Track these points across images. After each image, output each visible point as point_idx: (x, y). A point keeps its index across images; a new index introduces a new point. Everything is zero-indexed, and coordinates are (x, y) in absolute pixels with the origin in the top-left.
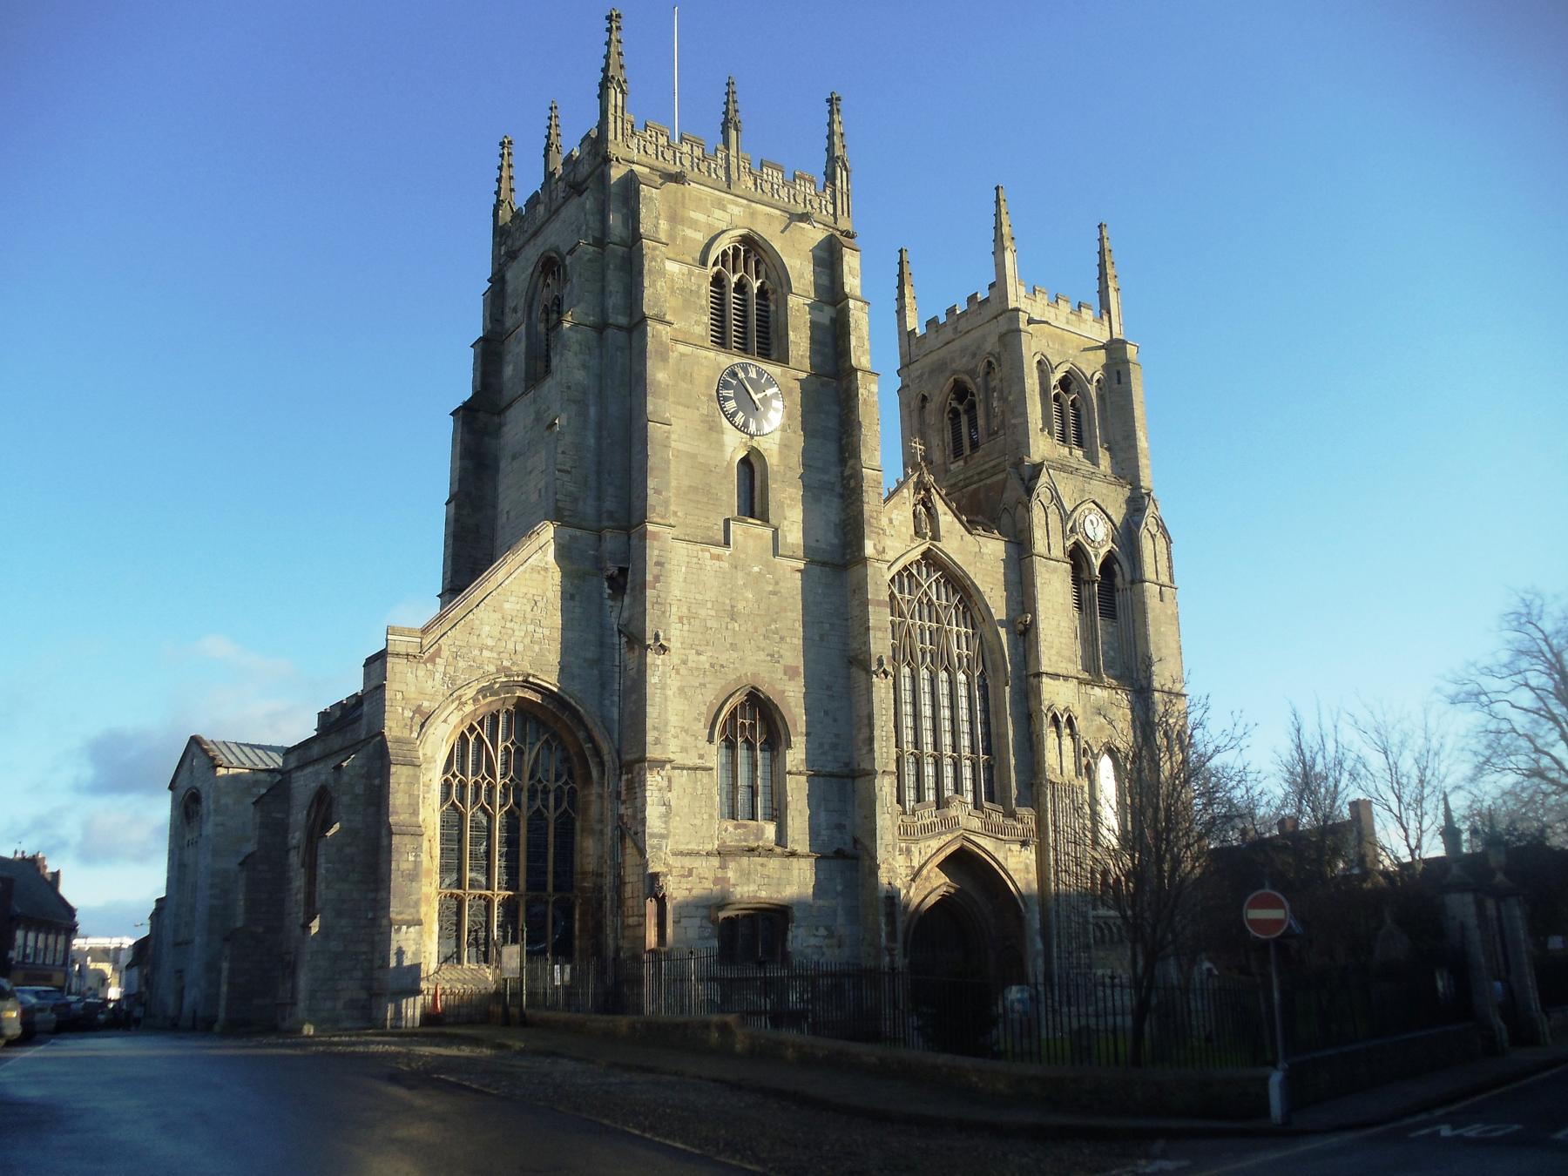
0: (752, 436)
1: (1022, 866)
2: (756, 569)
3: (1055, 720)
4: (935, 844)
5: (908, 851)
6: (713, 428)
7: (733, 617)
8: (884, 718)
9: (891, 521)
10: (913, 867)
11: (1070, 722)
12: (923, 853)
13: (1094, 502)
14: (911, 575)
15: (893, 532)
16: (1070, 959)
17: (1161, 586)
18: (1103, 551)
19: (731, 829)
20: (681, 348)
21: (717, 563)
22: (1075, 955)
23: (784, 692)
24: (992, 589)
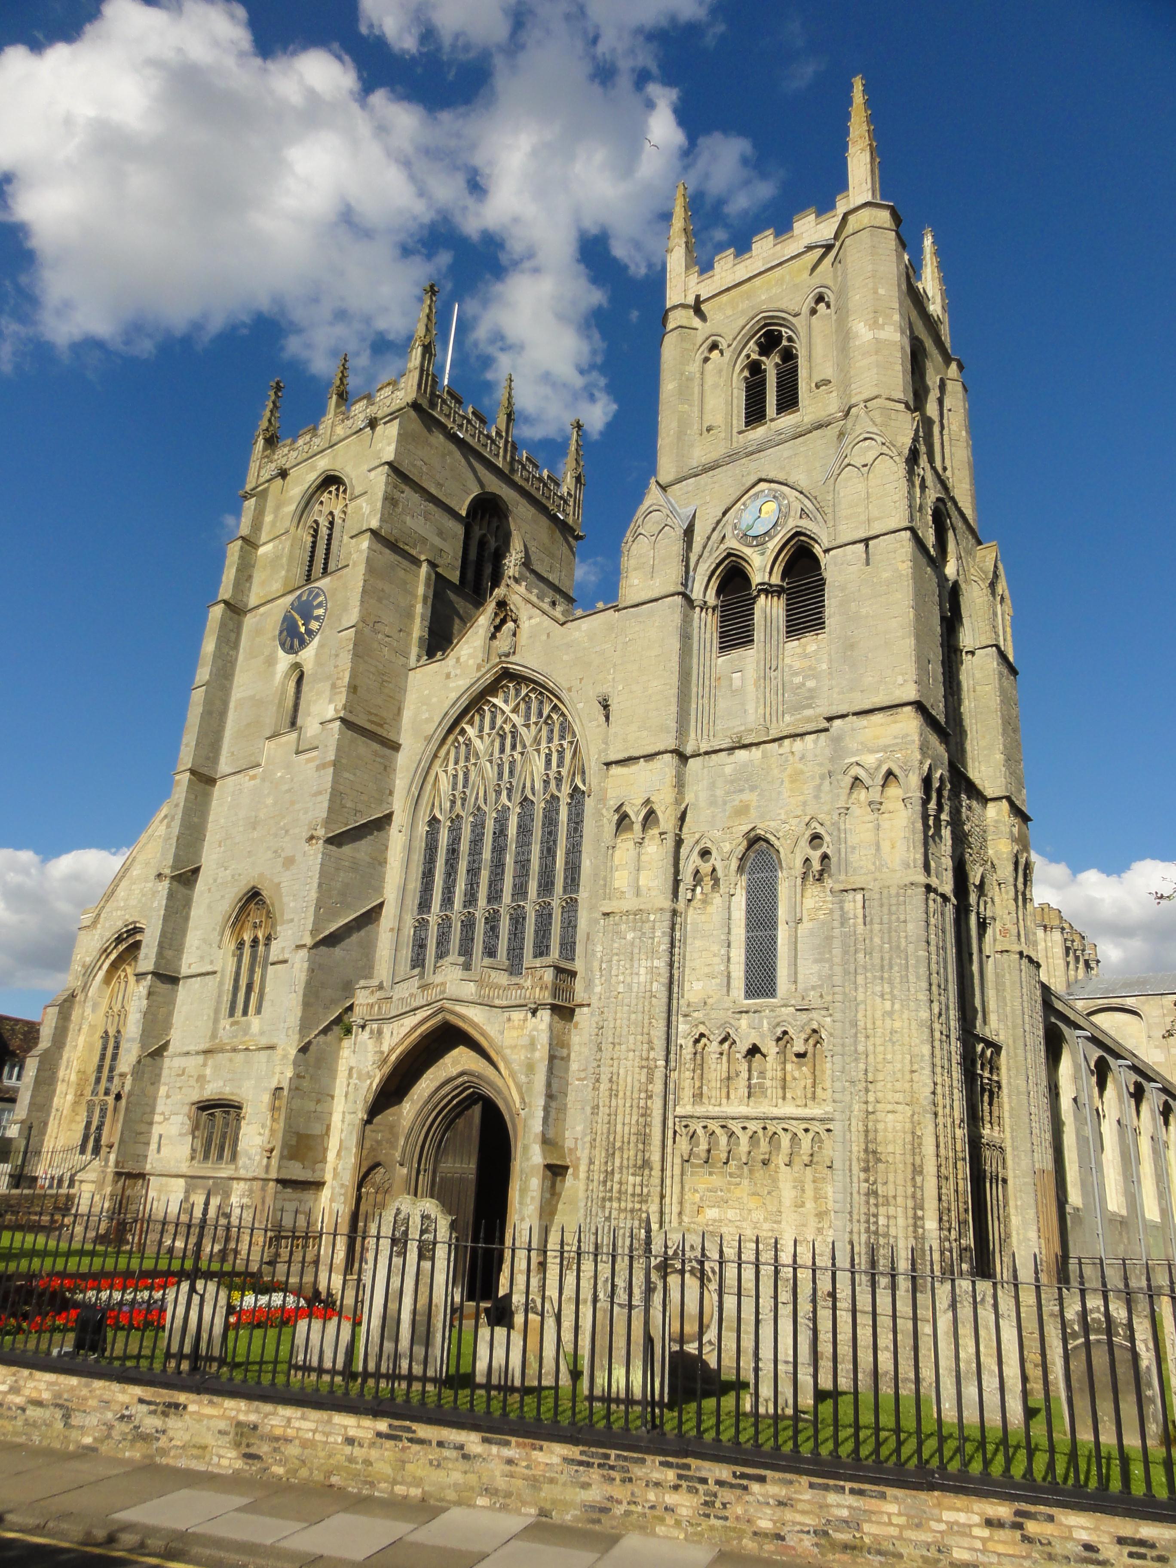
0: (296, 653)
1: (525, 1041)
2: (279, 774)
3: (623, 821)
4: (410, 1022)
5: (380, 1032)
6: (271, 661)
7: (254, 825)
8: (307, 887)
9: (458, 659)
10: (382, 1053)
11: (650, 817)
12: (395, 1033)
13: (761, 480)
14: (494, 705)
15: (458, 672)
16: (609, 1184)
17: (866, 541)
18: (773, 545)
19: (228, 1027)
20: (262, 610)
21: (253, 782)
22: (617, 1177)
23: (279, 883)
24: (581, 679)
